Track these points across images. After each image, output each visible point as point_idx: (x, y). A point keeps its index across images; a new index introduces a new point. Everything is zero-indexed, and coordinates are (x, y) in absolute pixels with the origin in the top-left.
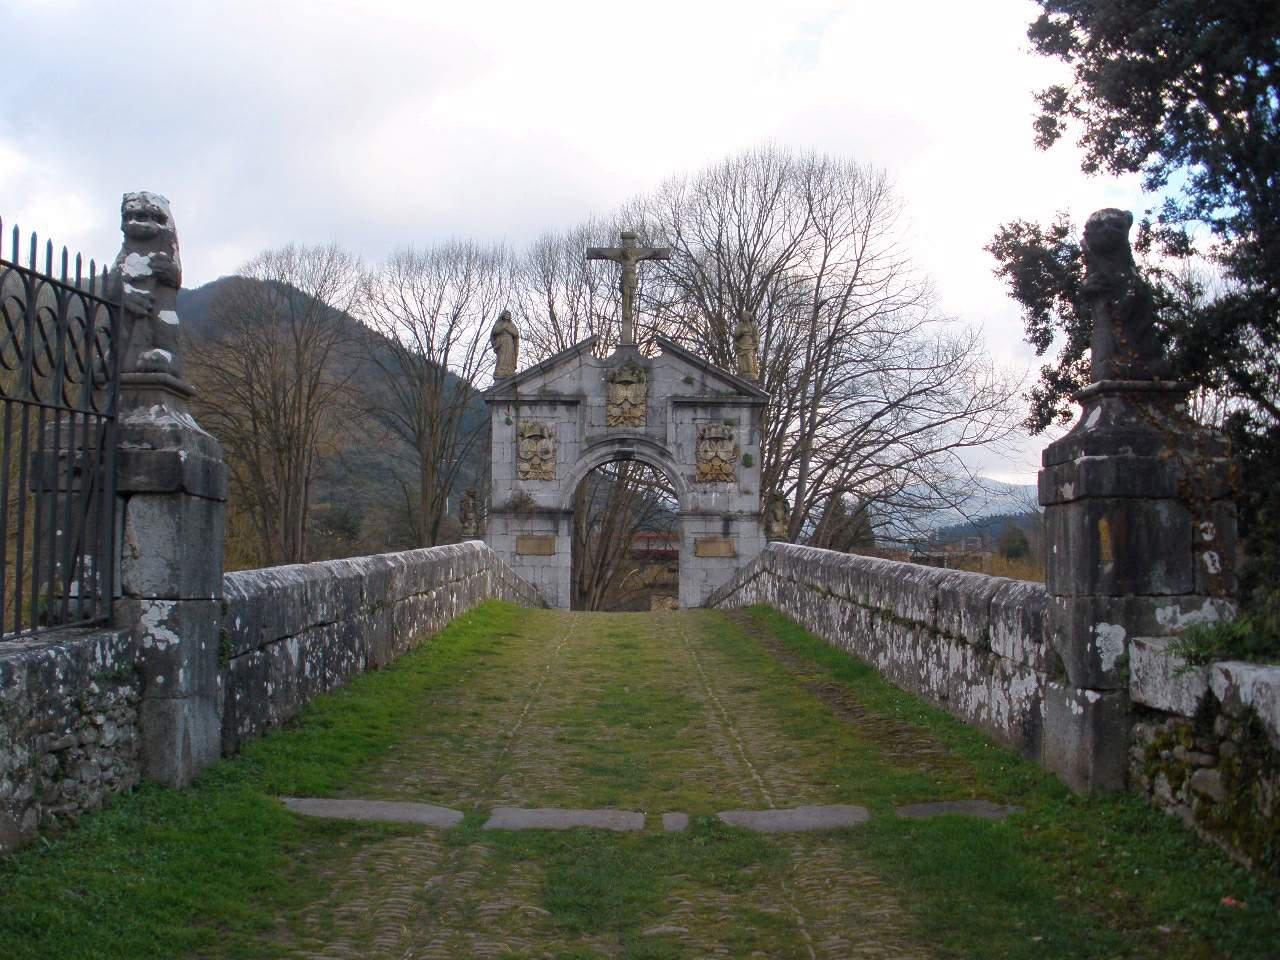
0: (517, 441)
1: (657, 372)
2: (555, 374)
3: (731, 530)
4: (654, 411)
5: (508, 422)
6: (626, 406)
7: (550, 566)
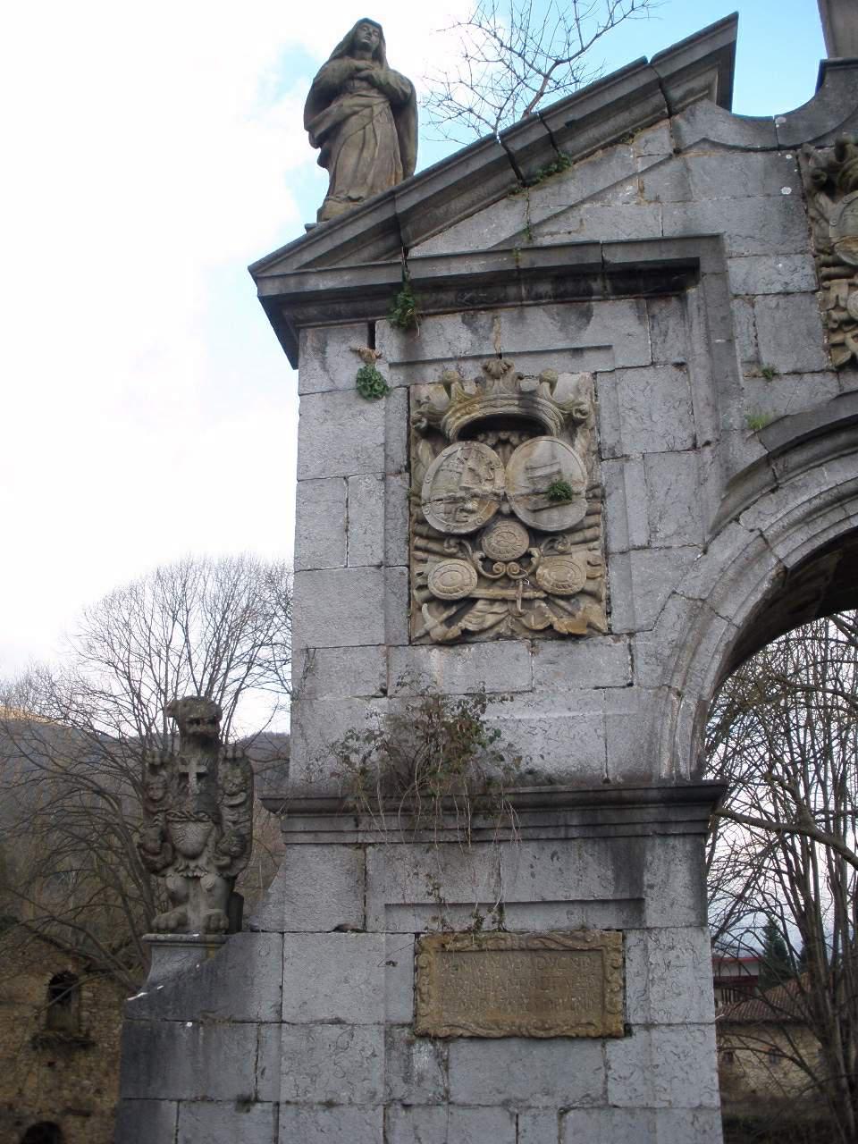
2: (576, 184)
5: (369, 388)
7: (602, 1103)
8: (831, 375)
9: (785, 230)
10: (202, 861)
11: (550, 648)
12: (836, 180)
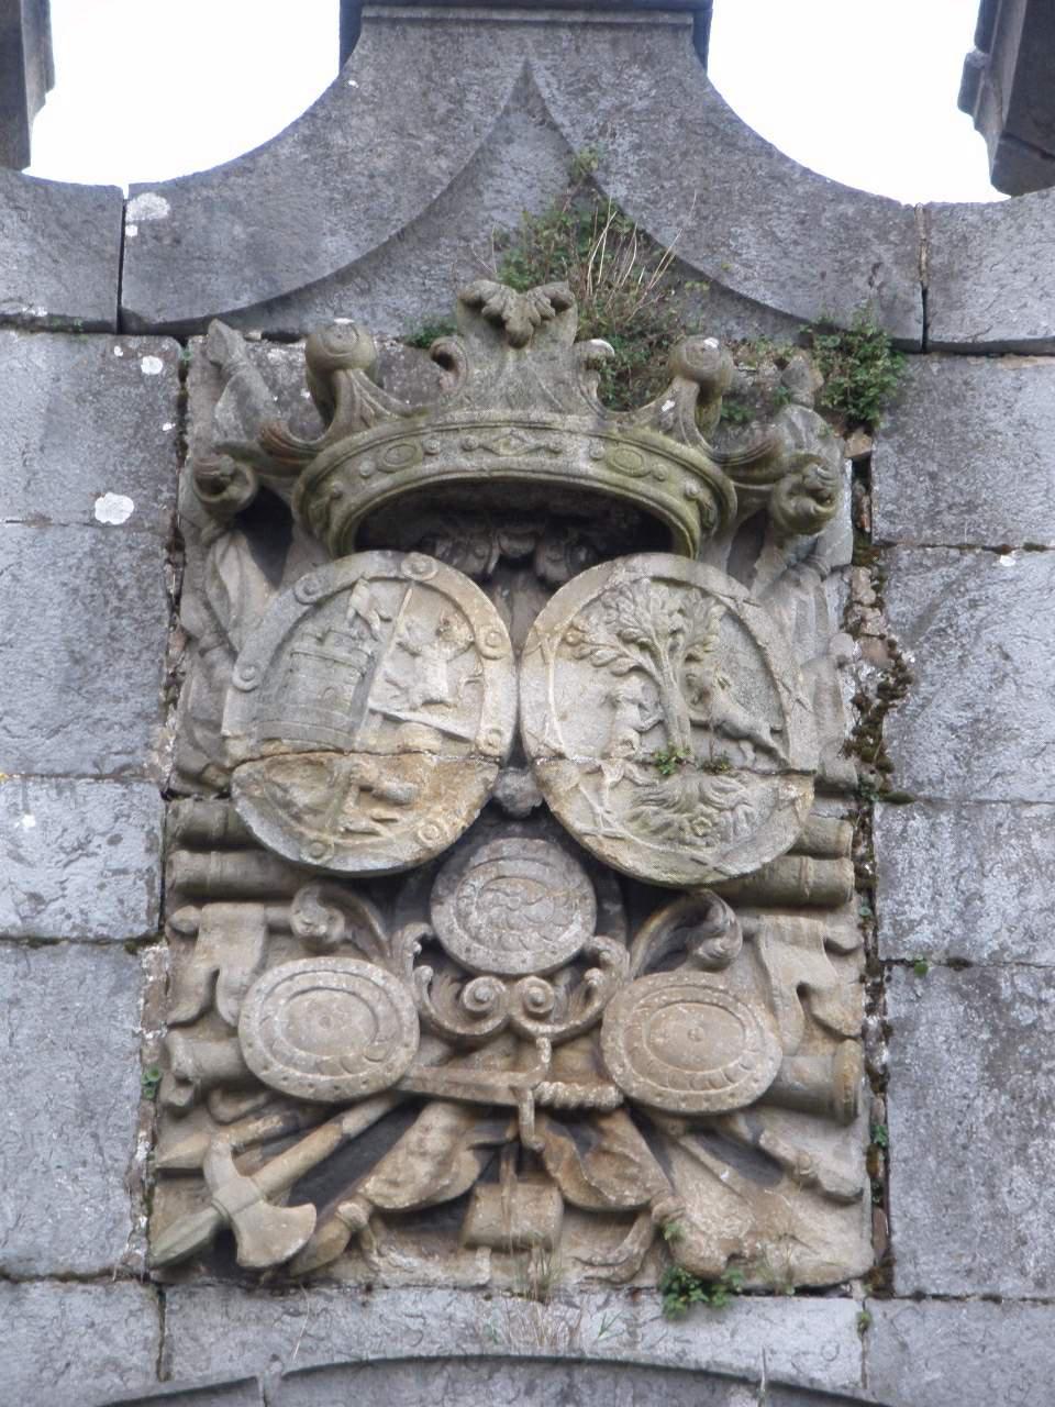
6: (521, 918)
9: (79, 673)
12: (292, 494)
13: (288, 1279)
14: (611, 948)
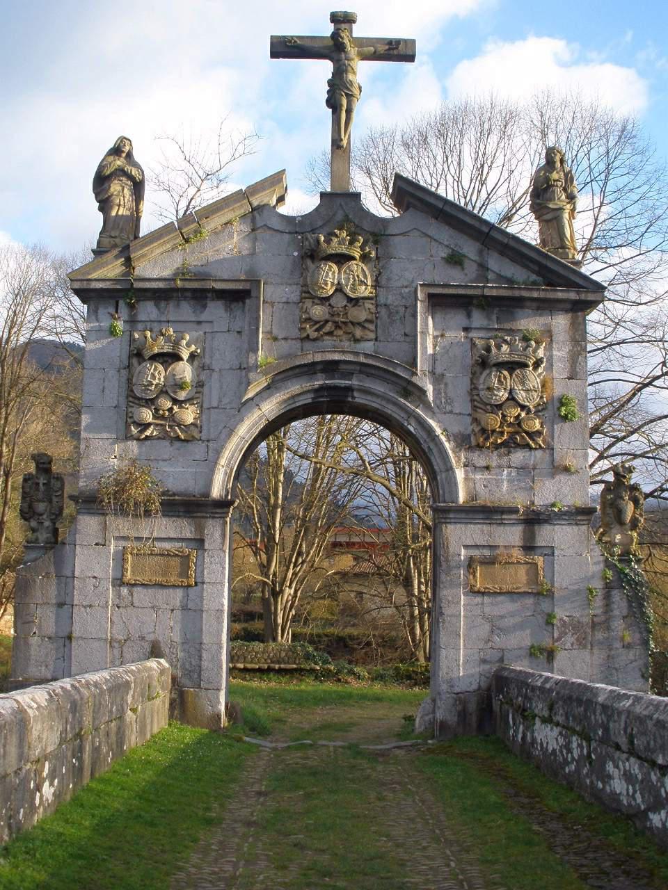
0: (129, 367)
1: (399, 246)
3: (540, 542)
4: (390, 315)
6: (339, 302)
8: (299, 341)
9: (292, 273)
10: (45, 517)
11: (177, 444)
13: (315, 340)
14: (349, 305)
